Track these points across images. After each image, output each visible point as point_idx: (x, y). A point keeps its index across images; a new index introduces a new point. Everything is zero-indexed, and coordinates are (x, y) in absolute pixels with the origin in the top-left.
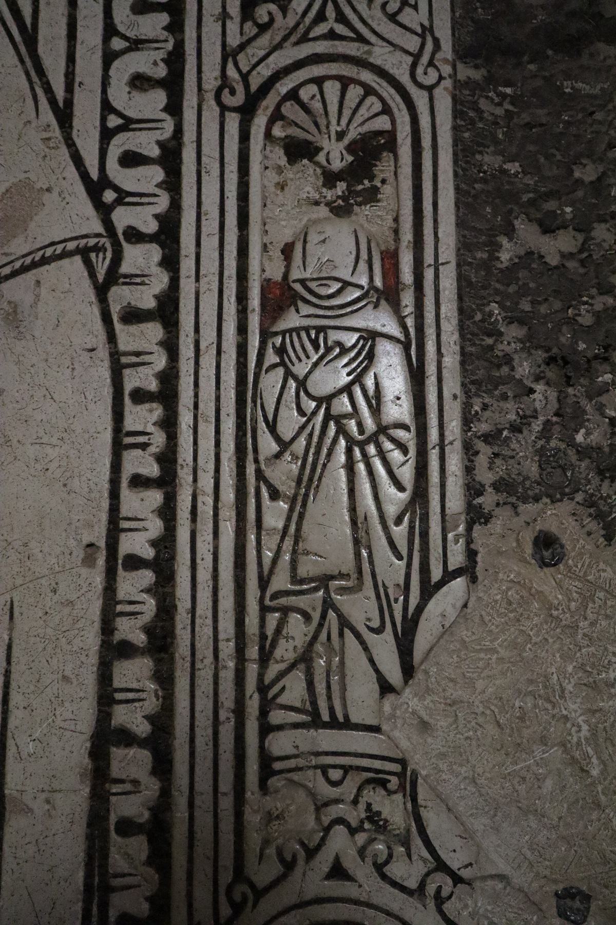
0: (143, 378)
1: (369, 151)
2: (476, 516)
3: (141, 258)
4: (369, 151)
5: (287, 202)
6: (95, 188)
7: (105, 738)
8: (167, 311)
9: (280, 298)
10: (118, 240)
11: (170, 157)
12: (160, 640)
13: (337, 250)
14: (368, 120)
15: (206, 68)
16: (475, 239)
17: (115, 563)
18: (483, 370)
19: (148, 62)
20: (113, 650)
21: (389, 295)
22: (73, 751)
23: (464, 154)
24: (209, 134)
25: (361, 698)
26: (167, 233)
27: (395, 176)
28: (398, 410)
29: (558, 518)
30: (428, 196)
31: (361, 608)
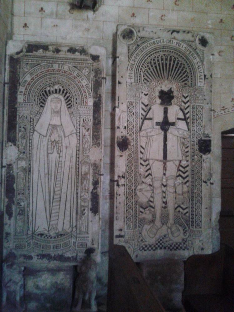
0: (78, 139)
1: (88, 129)
2: (92, 145)
3: (78, 134)
4: (88, 129)
5: (85, 131)
6: (76, 130)
7: (76, 154)
8: (79, 136)
9: (84, 136)
10: (77, 133)
11: (80, 129)
12: (79, 150)
13: (87, 133)
14: (88, 127)
15: (81, 125)
16: (93, 134)
17: (77, 147)
18: (93, 139)
19: (79, 124)
20: (77, 151)
21: (89, 136)
22: (75, 154)
23: (93, 130)
24: (81, 128)
25: (87, 153)
26: (79, 132)
27: (90, 130)
28: (89, 141)
29: (96, 146)
30: (91, 131)
31: (87, 149)
